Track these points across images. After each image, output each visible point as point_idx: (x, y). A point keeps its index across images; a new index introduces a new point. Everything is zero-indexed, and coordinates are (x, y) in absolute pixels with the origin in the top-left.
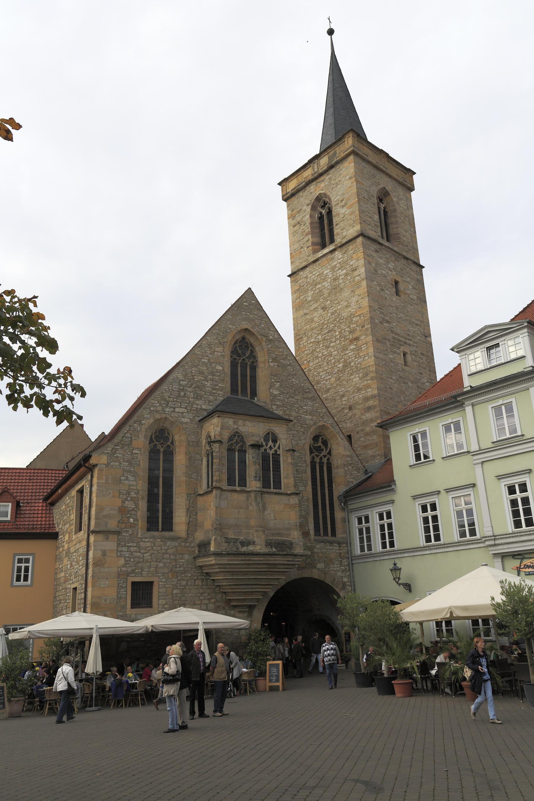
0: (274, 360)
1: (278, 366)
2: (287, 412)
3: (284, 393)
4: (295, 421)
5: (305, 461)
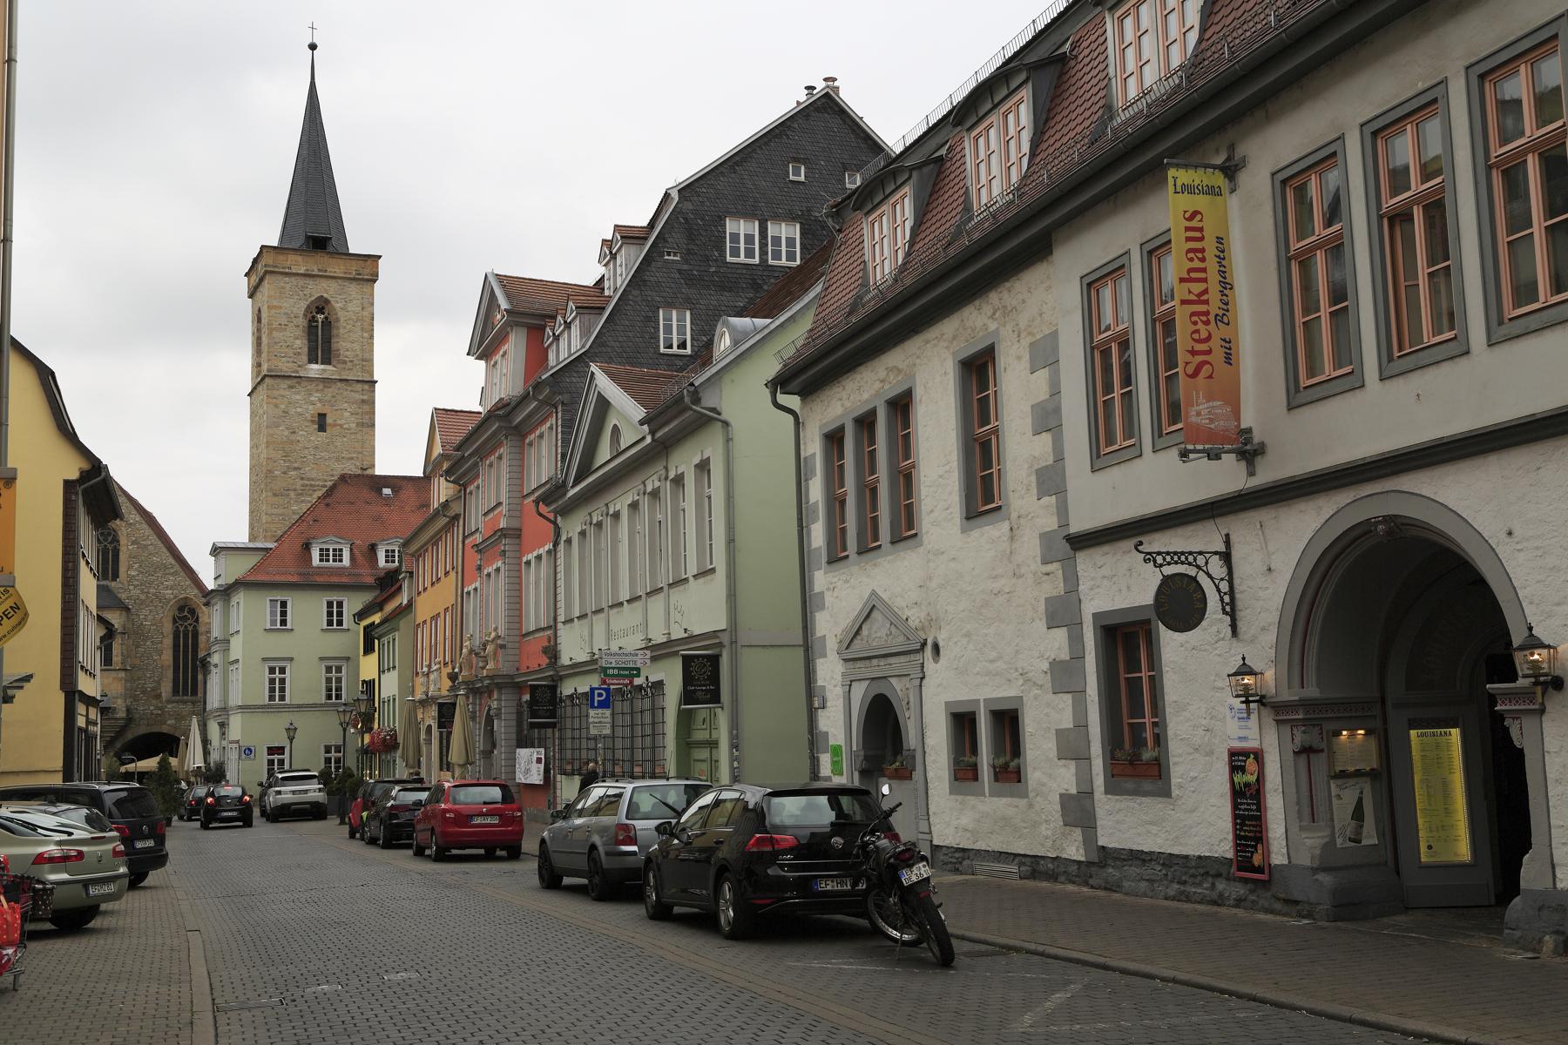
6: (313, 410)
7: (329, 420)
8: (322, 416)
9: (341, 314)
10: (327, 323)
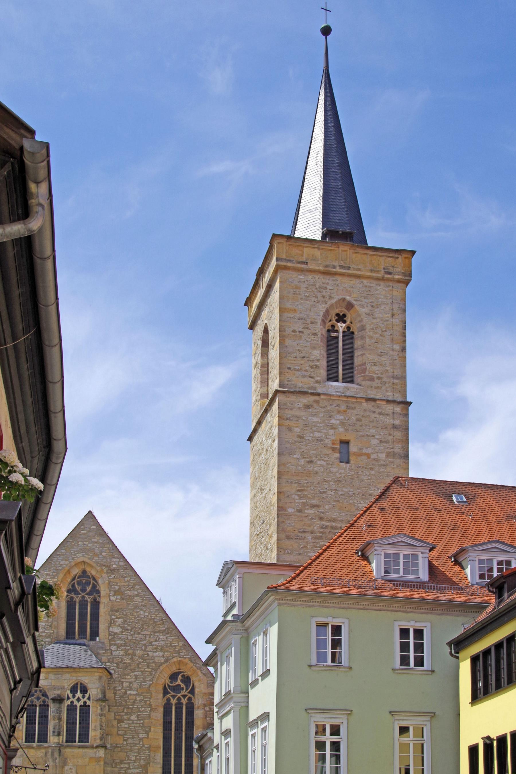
0: (116, 593)
1: (122, 599)
2: (130, 652)
3: (128, 629)
4: (140, 660)
5: (150, 705)
6: (333, 436)
7: (353, 448)
8: (345, 443)
9: (367, 321)
10: (349, 334)
